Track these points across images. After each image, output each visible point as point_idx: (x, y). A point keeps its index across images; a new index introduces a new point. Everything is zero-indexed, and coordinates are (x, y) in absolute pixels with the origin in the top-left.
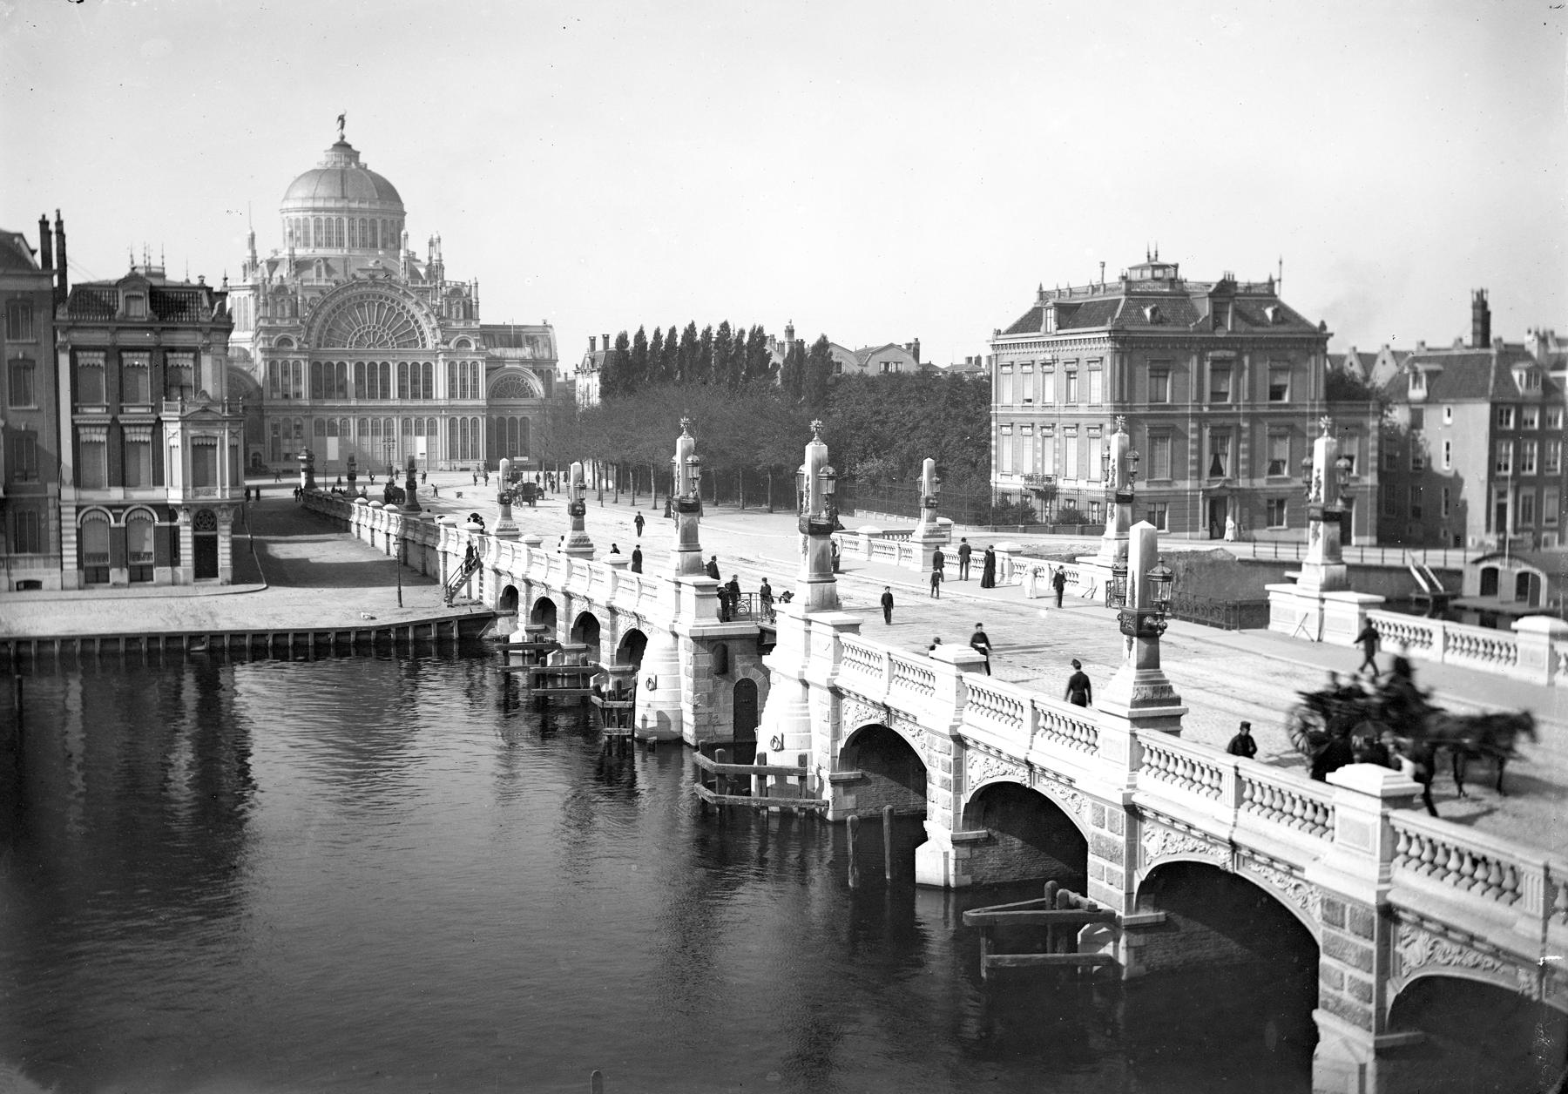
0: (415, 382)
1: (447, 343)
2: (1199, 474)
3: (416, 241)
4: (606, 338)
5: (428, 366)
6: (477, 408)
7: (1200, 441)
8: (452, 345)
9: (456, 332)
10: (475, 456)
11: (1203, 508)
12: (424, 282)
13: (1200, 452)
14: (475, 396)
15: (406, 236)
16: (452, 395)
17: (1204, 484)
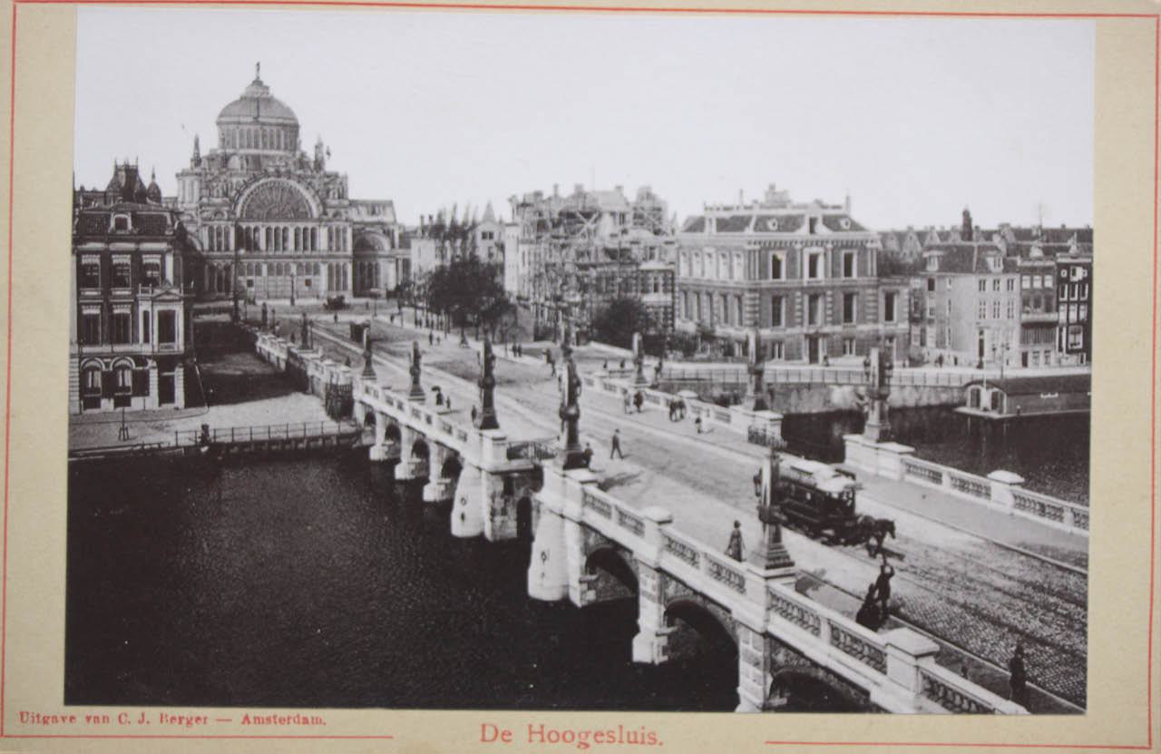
3: (307, 146)
4: (431, 218)
6: (346, 257)
7: (801, 303)
11: (805, 345)
12: (312, 171)
14: (345, 250)
15: (300, 142)
17: (805, 330)
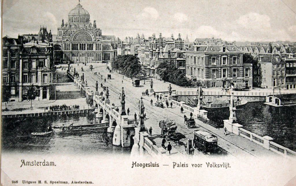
0: (90, 47)
1: (96, 40)
2: (221, 77)
5: (92, 44)
7: (221, 71)
8: (97, 41)
9: (98, 38)
10: (100, 60)
13: (221, 73)
16: (96, 50)
